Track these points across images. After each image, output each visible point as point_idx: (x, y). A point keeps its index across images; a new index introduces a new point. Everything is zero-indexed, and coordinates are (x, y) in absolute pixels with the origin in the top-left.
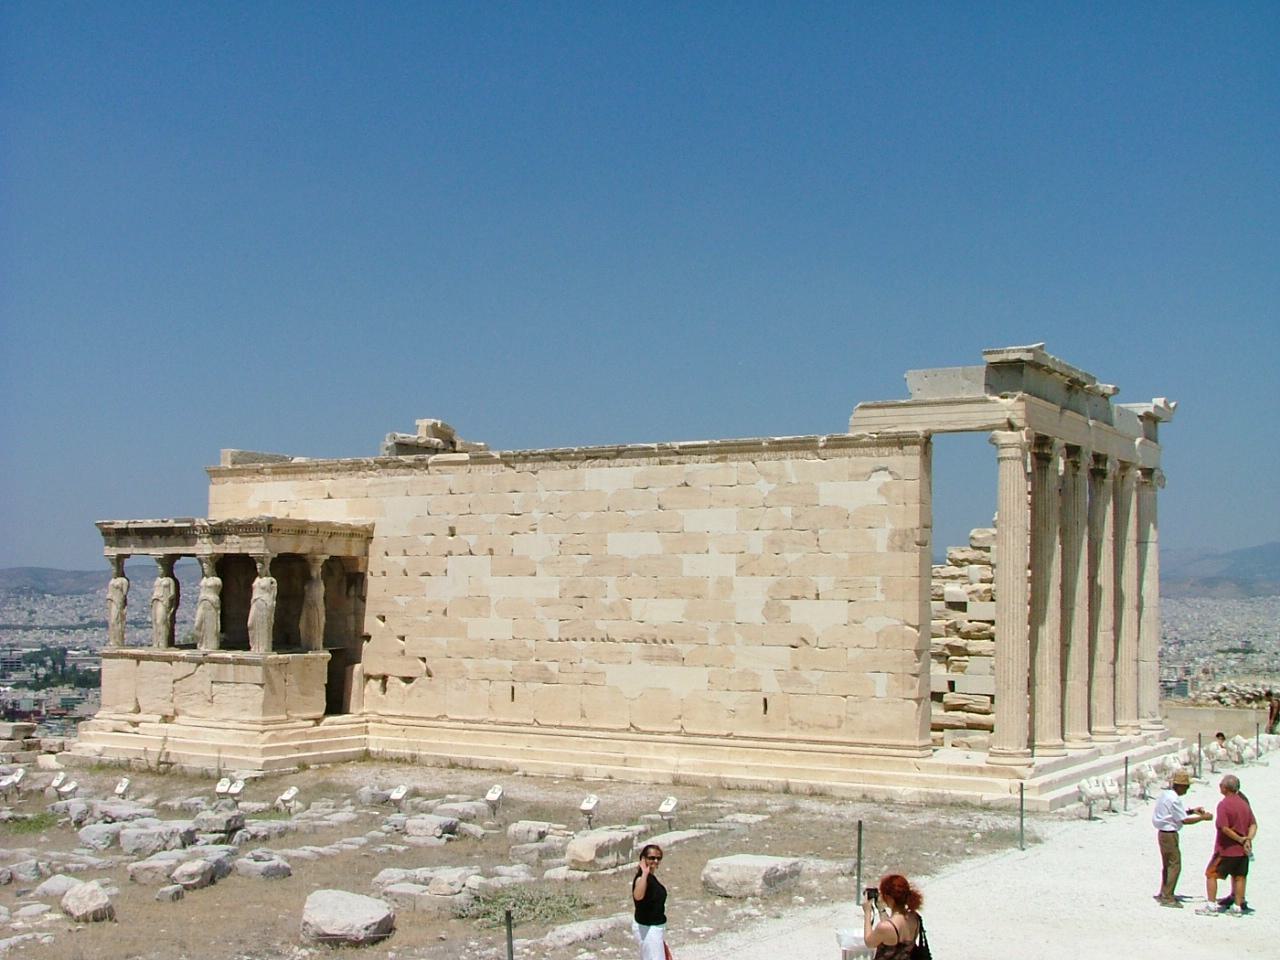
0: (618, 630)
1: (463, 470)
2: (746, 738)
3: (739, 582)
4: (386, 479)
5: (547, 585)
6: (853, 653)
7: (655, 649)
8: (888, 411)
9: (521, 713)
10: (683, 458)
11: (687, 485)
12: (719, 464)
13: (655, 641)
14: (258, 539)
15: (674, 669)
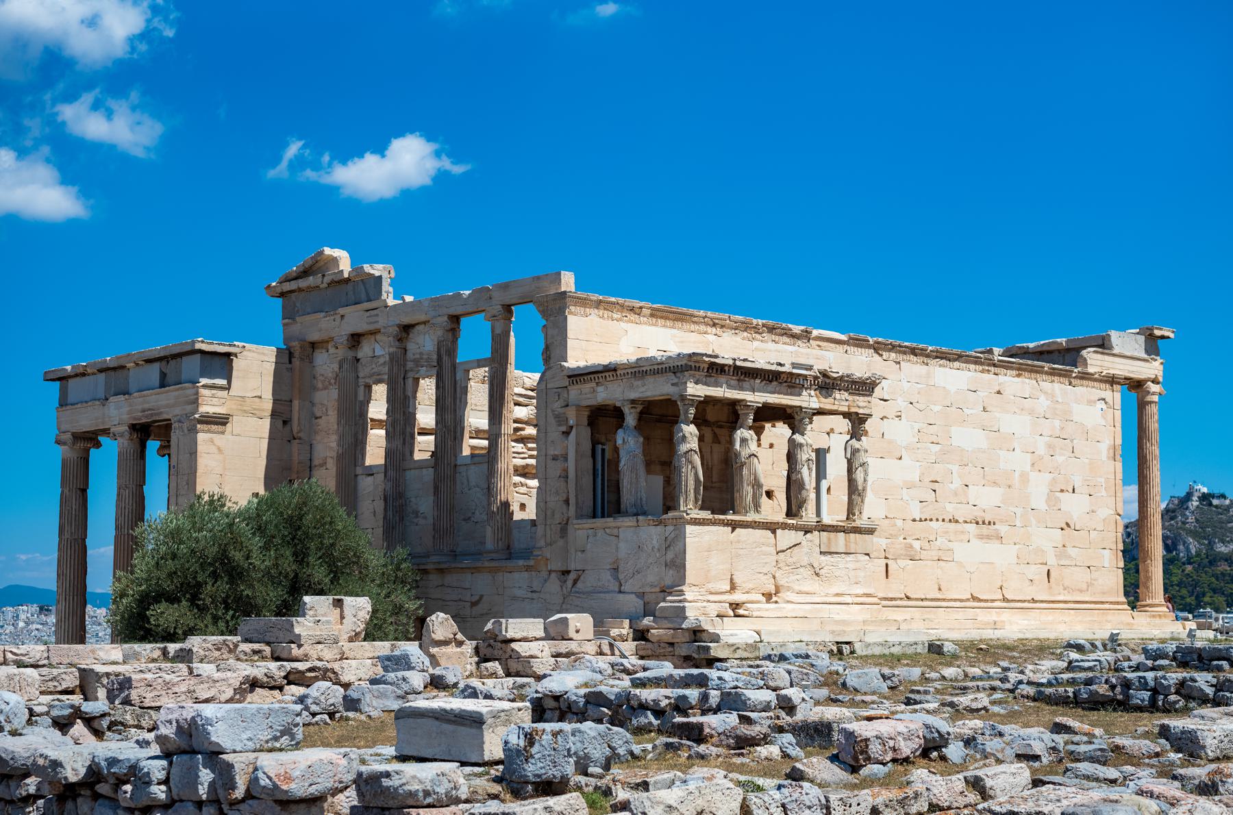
0: (962, 513)
1: (841, 348)
2: (1042, 601)
3: (1034, 476)
4: (771, 345)
5: (909, 470)
6: (1093, 534)
7: (985, 530)
8: (1106, 357)
9: (895, 589)
10: (997, 370)
11: (999, 392)
12: (1016, 379)
13: (984, 523)
14: (866, 399)
15: (994, 546)
